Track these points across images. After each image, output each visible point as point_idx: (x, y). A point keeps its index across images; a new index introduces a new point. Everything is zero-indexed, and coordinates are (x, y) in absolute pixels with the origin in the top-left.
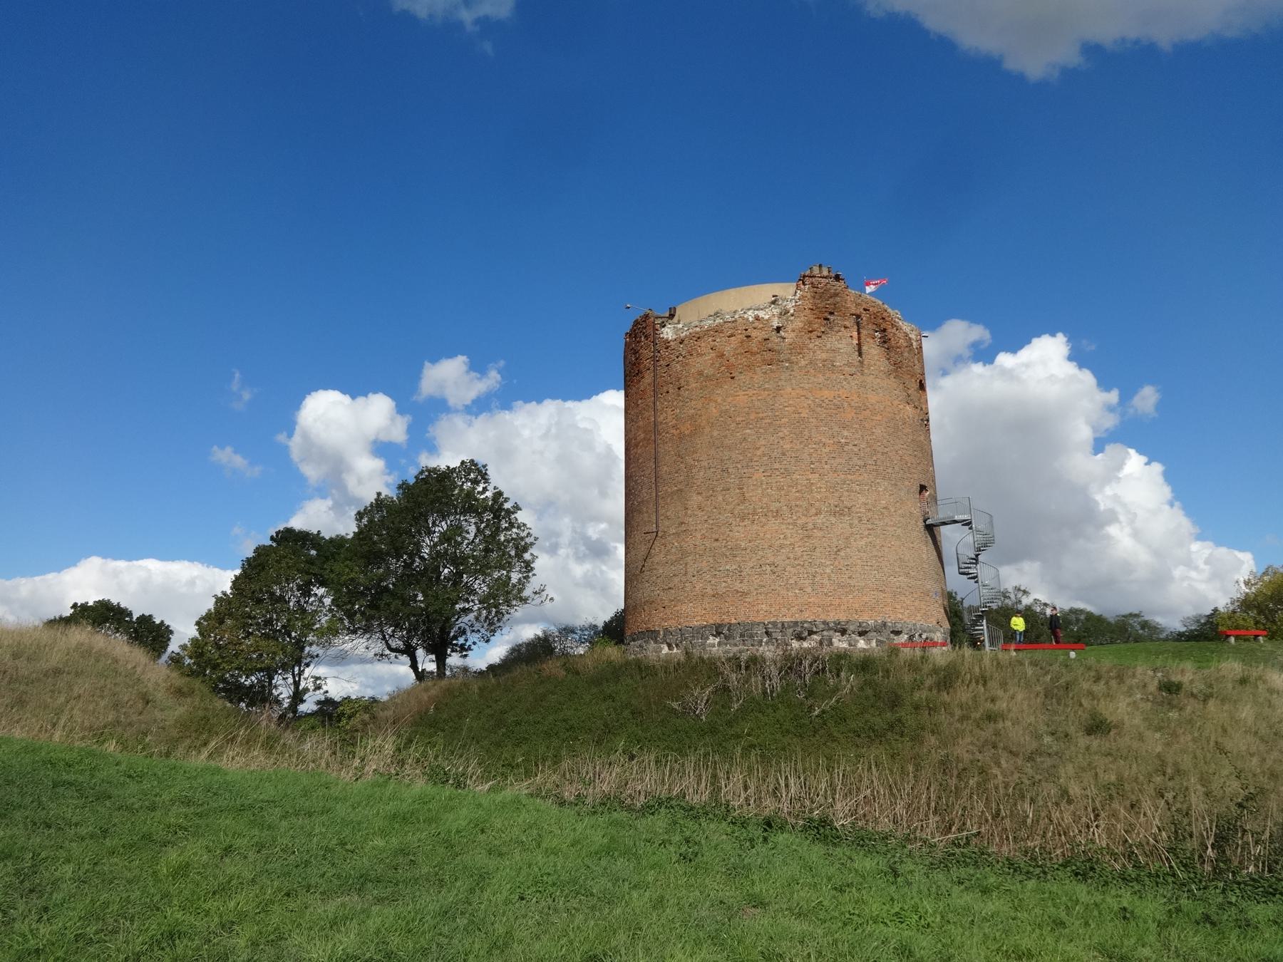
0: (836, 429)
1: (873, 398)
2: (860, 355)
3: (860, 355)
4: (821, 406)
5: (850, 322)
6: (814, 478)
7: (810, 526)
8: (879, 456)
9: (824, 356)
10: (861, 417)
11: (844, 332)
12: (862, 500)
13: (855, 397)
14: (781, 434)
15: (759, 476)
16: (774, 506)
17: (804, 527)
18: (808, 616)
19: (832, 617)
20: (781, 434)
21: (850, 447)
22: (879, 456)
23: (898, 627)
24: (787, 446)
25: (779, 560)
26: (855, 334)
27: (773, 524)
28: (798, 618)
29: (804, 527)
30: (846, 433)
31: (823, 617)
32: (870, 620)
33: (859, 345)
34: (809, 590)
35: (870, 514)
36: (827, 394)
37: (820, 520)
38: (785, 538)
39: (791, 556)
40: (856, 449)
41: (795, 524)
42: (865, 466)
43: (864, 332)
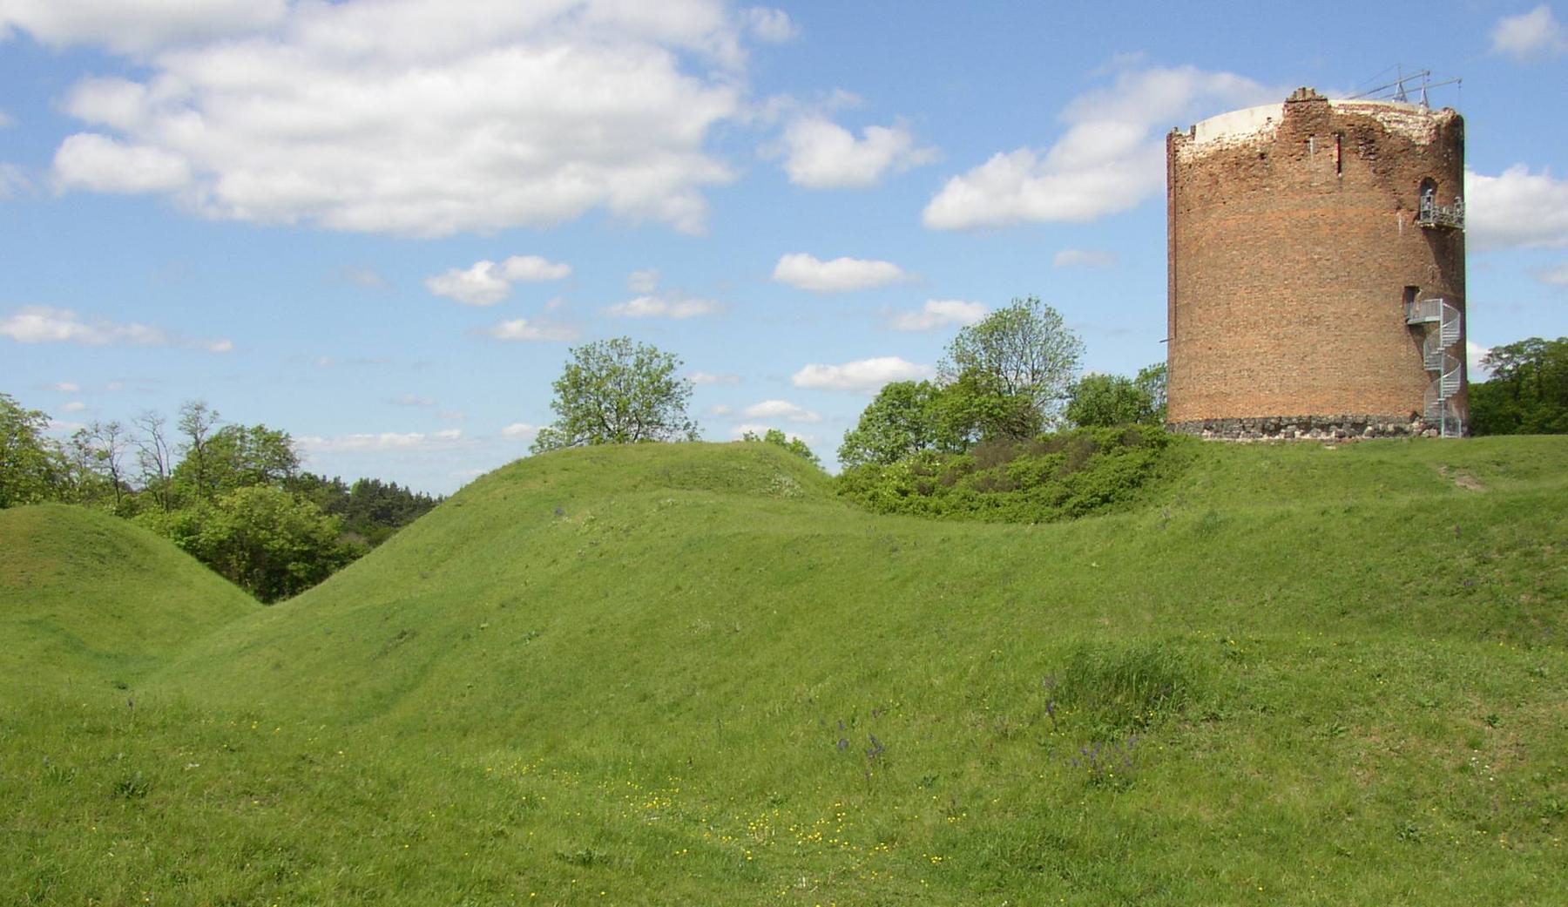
9: (1302, 178)
13: (1331, 215)
15: (1242, 293)
17: (1276, 337)
18: (1275, 413)
19: (1295, 414)
23: (1360, 420)
24: (1266, 265)
25: (1255, 366)
26: (1336, 152)
27: (1251, 336)
28: (1267, 414)
30: (1319, 249)
31: (1287, 414)
32: (1330, 415)
33: (1339, 162)
36: (1303, 214)
37: (1290, 330)
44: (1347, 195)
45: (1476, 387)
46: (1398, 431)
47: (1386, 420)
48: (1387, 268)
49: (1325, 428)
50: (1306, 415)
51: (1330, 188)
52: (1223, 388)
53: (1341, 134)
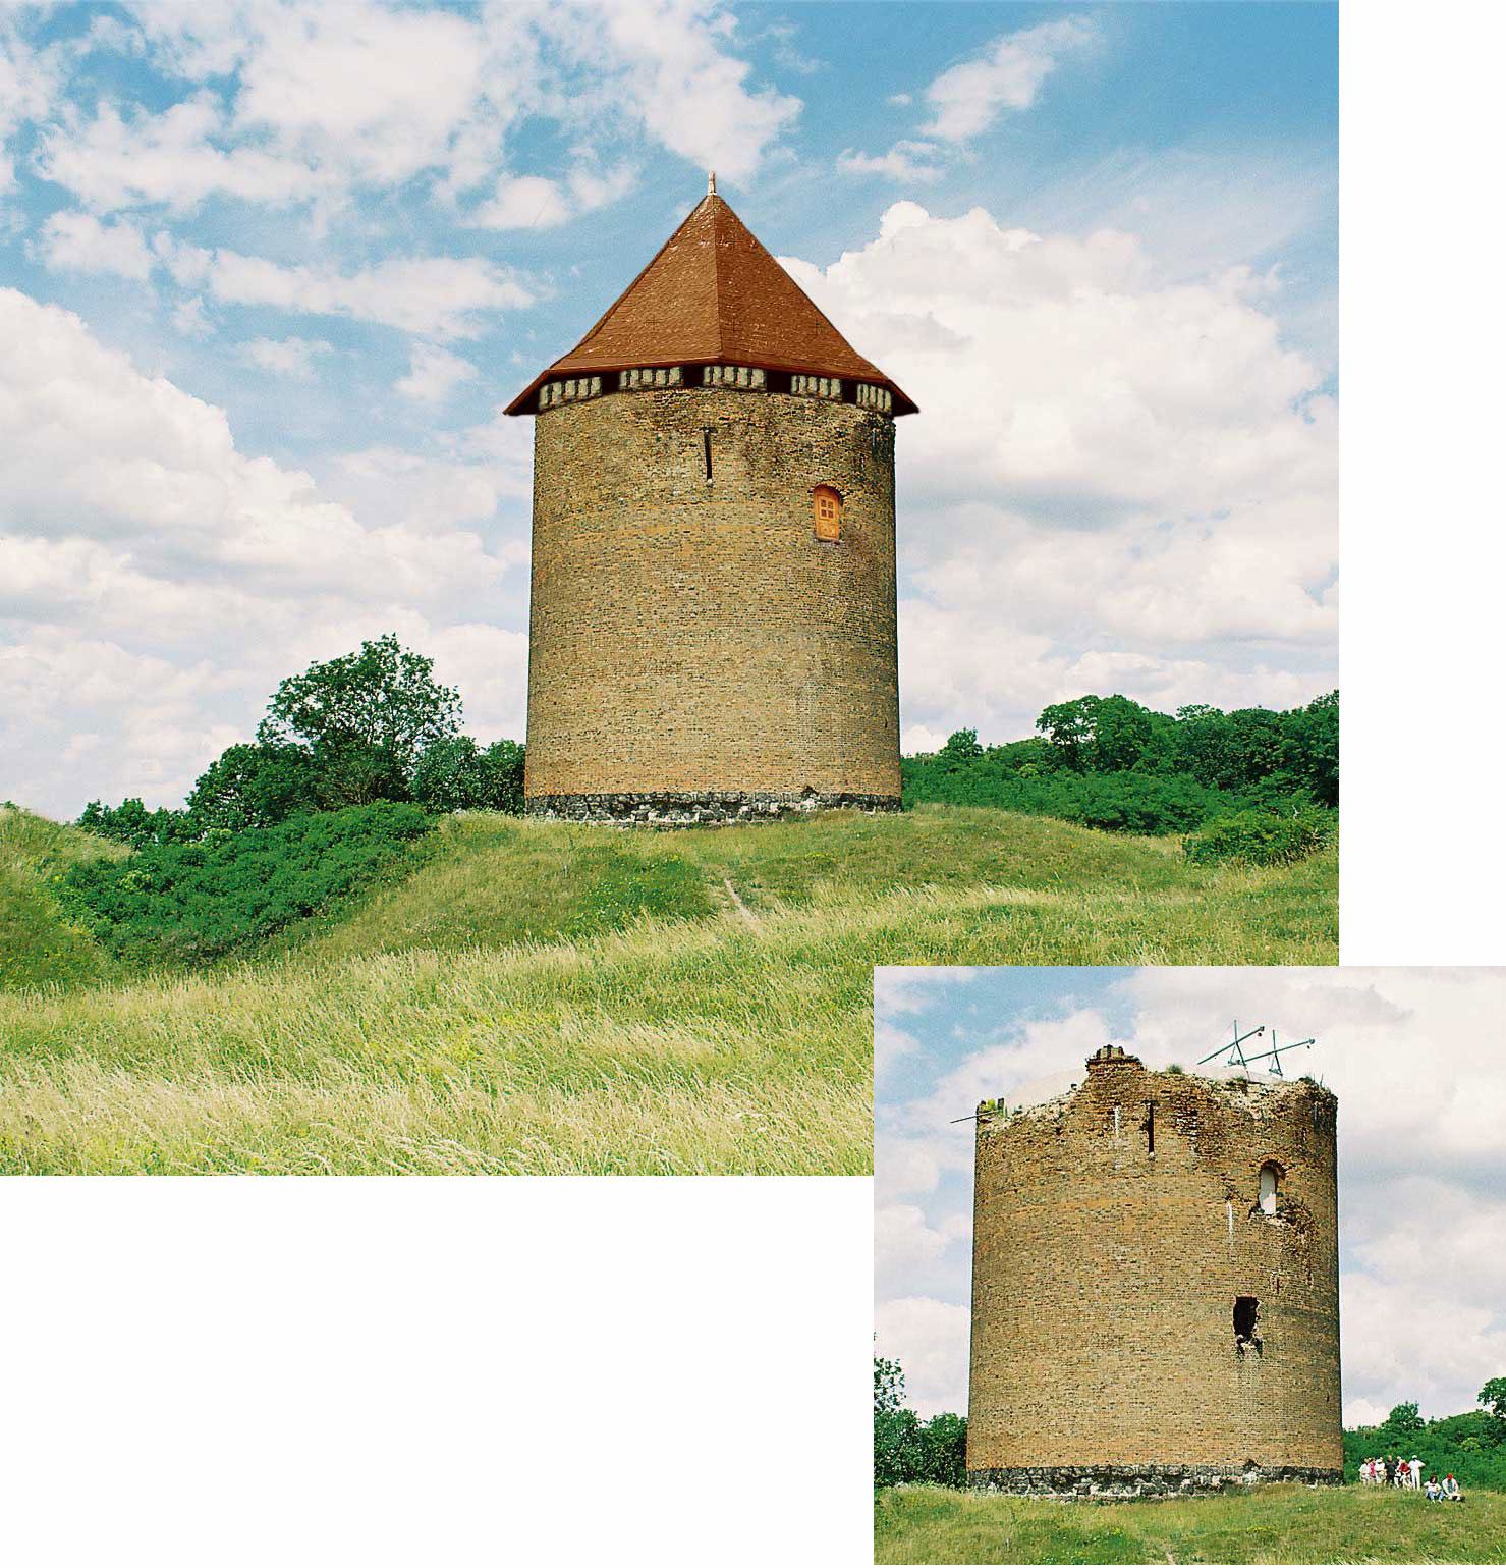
1: (723, 528)
2: (709, 476)
4: (654, 546)
6: (641, 631)
7: (633, 687)
8: (725, 598)
9: (662, 485)
10: (702, 554)
12: (696, 652)
14: (611, 583)
15: (589, 631)
16: (600, 665)
20: (611, 583)
21: (686, 591)
23: (731, 798)
24: (616, 596)
25: (600, 726)
28: (614, 789)
29: (627, 689)
30: (681, 575)
34: (627, 759)
37: (644, 679)
38: (608, 702)
39: (613, 721)
40: (692, 593)
41: (618, 685)
42: (704, 612)
45: (921, 761)
46: (784, 810)
47: (766, 797)
49: (686, 807)
50: (660, 791)
51: (697, 497)
52: (568, 756)
53: (712, 429)
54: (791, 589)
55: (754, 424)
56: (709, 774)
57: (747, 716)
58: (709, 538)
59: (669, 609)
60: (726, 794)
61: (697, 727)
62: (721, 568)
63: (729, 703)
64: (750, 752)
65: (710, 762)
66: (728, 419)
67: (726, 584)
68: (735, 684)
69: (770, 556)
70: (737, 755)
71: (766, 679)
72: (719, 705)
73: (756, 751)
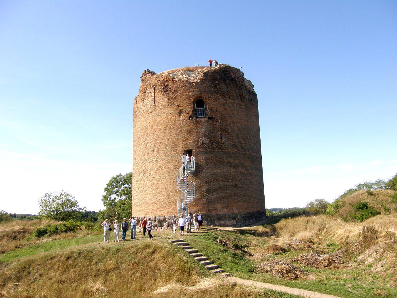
0: (145, 138)
3: (155, 103)
4: (142, 130)
5: (152, 90)
11: (150, 95)
22: (160, 144)
23: (162, 218)
30: (147, 138)
33: (155, 98)
35: (153, 171)
43: (157, 91)
44: (157, 112)
48: (174, 143)
54: (182, 137)
55: (168, 80)
56: (155, 210)
57: (166, 187)
58: (155, 124)
59: (145, 151)
60: (160, 217)
61: (152, 192)
62: (158, 133)
63: (161, 183)
64: (167, 201)
65: (155, 205)
66: (160, 80)
67: (159, 139)
68: (163, 175)
69: (174, 126)
70: (163, 202)
71: (173, 173)
72: (158, 184)
73: (170, 200)
